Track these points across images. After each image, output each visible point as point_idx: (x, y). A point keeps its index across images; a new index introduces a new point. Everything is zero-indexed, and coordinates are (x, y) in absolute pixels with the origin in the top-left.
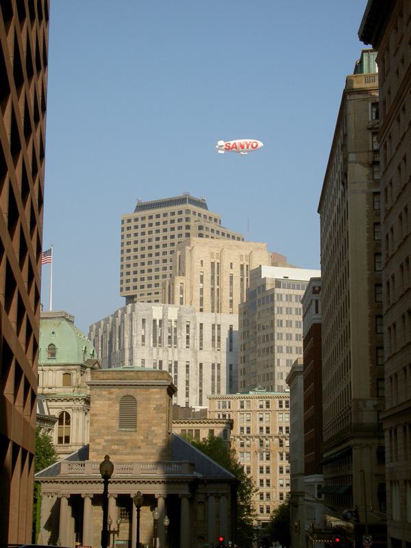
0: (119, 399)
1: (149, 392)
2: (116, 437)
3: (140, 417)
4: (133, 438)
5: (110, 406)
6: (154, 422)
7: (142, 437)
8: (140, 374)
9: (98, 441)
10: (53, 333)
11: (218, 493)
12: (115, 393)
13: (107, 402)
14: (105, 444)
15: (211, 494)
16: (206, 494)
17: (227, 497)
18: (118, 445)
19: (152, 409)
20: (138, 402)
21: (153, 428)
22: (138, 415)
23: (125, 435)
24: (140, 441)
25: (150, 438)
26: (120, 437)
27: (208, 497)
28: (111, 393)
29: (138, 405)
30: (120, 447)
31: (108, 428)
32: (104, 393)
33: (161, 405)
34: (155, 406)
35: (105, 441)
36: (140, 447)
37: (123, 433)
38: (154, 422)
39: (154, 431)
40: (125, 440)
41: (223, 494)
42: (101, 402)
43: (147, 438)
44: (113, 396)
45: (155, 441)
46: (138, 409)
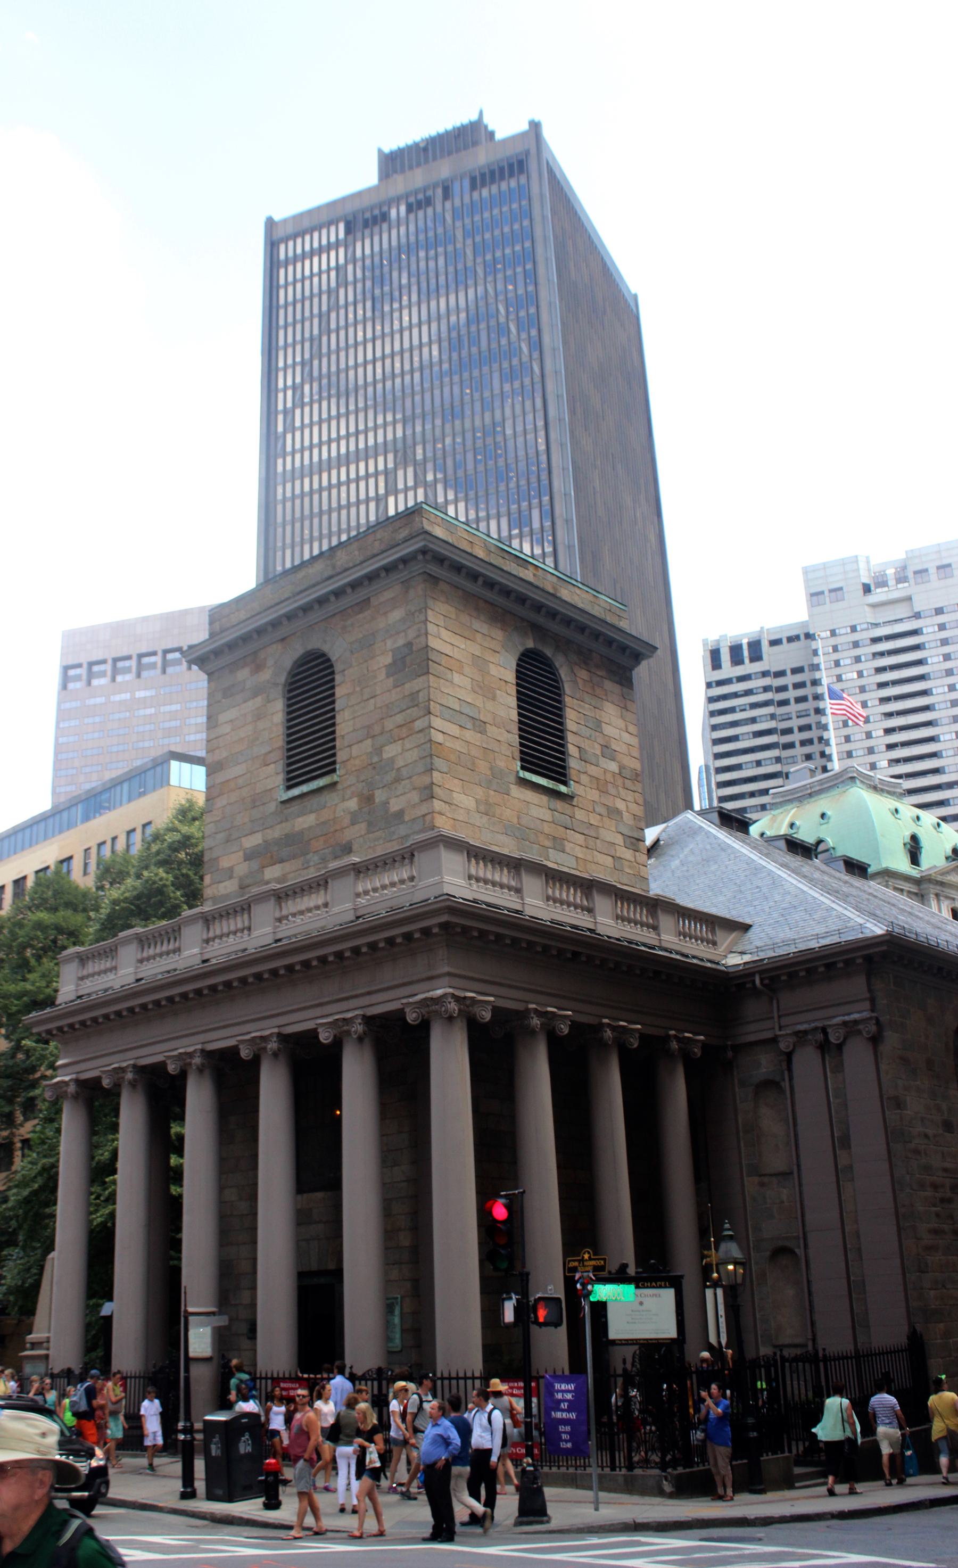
0: (282, 679)
1: (367, 613)
2: (276, 833)
3: (345, 725)
4: (326, 815)
5: (259, 716)
6: (389, 724)
7: (353, 804)
8: (342, 559)
9: (225, 863)
10: (823, 816)
11: (824, 1030)
12: (270, 662)
13: (250, 703)
14: (242, 869)
15: (801, 1036)
16: (774, 1040)
17: (875, 1040)
18: (282, 861)
19: (382, 675)
20: (338, 667)
21: (390, 751)
22: (339, 719)
23: (302, 814)
24: (347, 821)
25: (380, 796)
26: (286, 828)
27: (789, 1056)
28: (258, 668)
29: (338, 678)
30: (288, 867)
31: (255, 801)
32: (243, 674)
33: (409, 644)
34: (388, 659)
35: (249, 856)
36: (348, 849)
37: (295, 808)
38: (389, 724)
39: (392, 760)
40: (301, 833)
41: (851, 1028)
42: (232, 714)
43: (368, 799)
44: (266, 675)
45: (395, 806)
46: (339, 692)
